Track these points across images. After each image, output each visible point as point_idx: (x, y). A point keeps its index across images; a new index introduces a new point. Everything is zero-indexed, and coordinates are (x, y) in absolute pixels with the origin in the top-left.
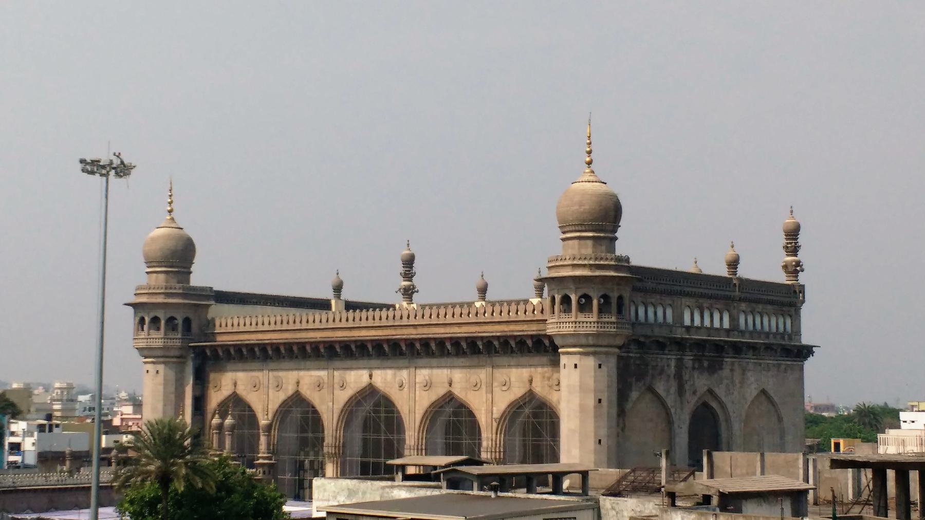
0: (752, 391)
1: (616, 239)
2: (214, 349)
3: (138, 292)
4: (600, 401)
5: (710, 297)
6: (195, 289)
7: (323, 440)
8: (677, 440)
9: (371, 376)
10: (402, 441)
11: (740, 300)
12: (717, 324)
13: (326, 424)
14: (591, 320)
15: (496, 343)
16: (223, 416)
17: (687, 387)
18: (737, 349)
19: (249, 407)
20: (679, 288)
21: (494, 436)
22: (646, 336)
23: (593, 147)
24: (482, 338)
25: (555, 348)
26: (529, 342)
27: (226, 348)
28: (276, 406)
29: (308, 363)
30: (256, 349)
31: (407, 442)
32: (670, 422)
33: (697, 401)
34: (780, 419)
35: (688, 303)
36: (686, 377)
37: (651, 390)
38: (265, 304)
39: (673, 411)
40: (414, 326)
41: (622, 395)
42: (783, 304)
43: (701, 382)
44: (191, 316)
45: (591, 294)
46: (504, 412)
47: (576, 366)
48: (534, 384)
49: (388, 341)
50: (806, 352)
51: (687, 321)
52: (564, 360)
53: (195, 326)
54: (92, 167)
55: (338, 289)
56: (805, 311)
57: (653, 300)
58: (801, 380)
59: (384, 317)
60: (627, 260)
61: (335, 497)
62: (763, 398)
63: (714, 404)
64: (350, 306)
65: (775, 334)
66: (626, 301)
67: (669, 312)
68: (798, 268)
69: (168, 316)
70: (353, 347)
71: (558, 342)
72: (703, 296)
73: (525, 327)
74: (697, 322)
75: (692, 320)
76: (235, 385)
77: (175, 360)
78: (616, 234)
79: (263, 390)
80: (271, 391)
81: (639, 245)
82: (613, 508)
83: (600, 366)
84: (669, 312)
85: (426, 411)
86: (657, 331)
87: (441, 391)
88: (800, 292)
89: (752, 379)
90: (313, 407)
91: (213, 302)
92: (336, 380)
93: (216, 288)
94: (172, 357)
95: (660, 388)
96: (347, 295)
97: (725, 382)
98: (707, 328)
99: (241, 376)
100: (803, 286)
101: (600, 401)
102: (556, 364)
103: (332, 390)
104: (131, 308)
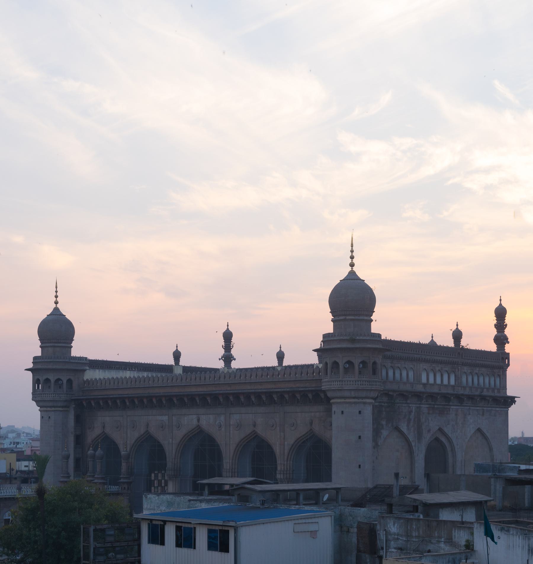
1: (372, 321)
3: (37, 361)
5: (441, 362)
6: (75, 358)
9: (198, 420)
11: (463, 364)
12: (446, 382)
13: (167, 454)
15: (286, 396)
16: (95, 450)
19: (114, 442)
21: (285, 463)
22: (394, 391)
24: (277, 392)
25: (328, 399)
26: (310, 396)
31: (225, 467)
37: (397, 429)
38: (125, 369)
39: (413, 444)
40: (229, 385)
41: (377, 432)
43: (433, 423)
44: (72, 378)
45: (353, 361)
46: (293, 445)
47: (342, 412)
49: (210, 395)
51: (424, 380)
52: (334, 408)
53: (75, 385)
56: (510, 371)
57: (399, 365)
60: (379, 335)
61: (159, 507)
63: (443, 439)
65: (488, 389)
67: (411, 374)
68: (505, 341)
69: (56, 378)
70: (186, 399)
71: (329, 394)
74: (431, 381)
75: (428, 379)
76: (104, 427)
79: (124, 429)
82: (351, 515)
83: (360, 412)
84: (411, 374)
85: (238, 445)
90: (159, 442)
91: (88, 368)
93: (91, 357)
94: (60, 407)
95: (404, 428)
96: (183, 362)
98: (438, 385)
100: (509, 354)
101: (360, 437)
102: (329, 412)
104: (30, 373)
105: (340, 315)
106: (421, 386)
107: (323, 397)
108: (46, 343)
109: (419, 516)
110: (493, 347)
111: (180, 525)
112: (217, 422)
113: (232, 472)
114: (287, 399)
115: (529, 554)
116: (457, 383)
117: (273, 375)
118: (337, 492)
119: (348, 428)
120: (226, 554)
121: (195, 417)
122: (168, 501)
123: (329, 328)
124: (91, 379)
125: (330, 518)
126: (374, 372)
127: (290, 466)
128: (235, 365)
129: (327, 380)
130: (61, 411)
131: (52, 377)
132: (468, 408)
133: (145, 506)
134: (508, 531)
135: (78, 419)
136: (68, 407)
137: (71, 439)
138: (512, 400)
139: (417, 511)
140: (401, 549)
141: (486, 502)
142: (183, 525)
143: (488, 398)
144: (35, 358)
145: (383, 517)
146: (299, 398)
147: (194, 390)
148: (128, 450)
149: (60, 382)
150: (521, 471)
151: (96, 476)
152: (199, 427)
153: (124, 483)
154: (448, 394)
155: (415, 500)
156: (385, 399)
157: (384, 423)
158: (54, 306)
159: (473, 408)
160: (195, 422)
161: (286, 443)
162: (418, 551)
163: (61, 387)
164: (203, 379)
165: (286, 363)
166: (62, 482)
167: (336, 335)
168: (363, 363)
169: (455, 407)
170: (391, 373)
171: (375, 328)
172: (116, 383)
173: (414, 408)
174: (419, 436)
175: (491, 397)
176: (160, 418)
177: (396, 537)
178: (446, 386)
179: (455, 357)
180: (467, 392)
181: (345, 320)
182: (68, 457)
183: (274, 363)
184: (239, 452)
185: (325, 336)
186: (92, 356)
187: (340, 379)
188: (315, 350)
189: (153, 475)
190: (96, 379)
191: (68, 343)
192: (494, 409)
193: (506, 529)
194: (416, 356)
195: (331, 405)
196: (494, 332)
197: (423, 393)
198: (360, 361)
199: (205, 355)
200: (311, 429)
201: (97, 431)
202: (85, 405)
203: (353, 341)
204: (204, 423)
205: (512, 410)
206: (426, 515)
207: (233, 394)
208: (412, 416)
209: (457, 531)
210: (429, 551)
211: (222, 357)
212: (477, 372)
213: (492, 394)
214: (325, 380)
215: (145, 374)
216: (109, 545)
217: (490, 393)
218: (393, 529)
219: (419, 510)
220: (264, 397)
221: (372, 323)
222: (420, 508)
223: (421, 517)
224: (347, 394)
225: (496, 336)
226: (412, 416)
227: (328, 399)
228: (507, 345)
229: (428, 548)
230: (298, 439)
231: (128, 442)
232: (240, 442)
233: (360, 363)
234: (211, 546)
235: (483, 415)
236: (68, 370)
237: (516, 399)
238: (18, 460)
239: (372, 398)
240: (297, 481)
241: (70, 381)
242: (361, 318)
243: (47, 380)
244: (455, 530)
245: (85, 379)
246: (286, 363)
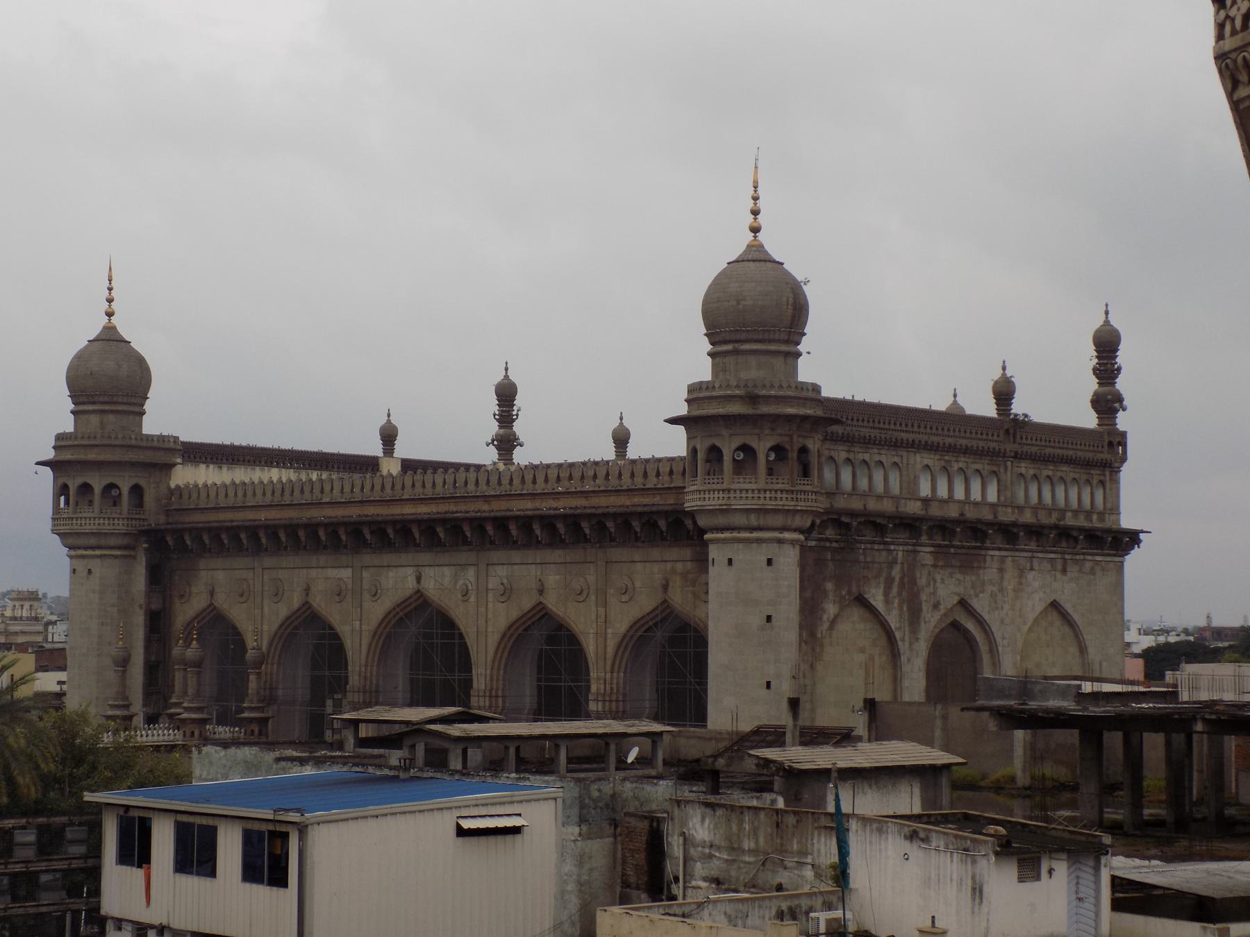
0: (1035, 604)
2: (179, 533)
3: (62, 443)
5: (966, 451)
6: (150, 438)
7: (347, 677)
8: (906, 683)
9: (419, 579)
10: (467, 684)
11: (1017, 456)
12: (976, 495)
13: (349, 654)
14: (754, 486)
15: (610, 524)
17: (924, 597)
18: (1010, 534)
19: (235, 628)
20: (911, 437)
21: (608, 675)
22: (853, 514)
23: (761, 204)
26: (662, 524)
27: (197, 532)
28: (275, 626)
29: (323, 559)
30: (243, 536)
31: (475, 685)
32: (894, 654)
33: (940, 620)
34: (1083, 650)
35: (926, 461)
36: (922, 581)
39: (898, 635)
42: (1088, 464)
43: (945, 589)
44: (142, 483)
45: (754, 445)
46: (625, 635)
47: (730, 561)
48: (670, 589)
49: (444, 521)
52: (713, 552)
53: (149, 498)
55: (389, 437)
56: (1128, 474)
57: (867, 457)
58: (1118, 586)
59: (439, 480)
60: (816, 388)
62: (1054, 616)
63: (970, 625)
64: (409, 466)
65: (1076, 513)
66: (814, 460)
67: (894, 478)
68: (1117, 405)
70: (390, 531)
71: (702, 522)
72: (951, 449)
73: (656, 499)
74: (943, 492)
75: (934, 489)
76: (212, 593)
77: (118, 553)
79: (254, 600)
80: (266, 602)
81: (834, 363)
83: (770, 562)
84: (894, 478)
85: (504, 635)
86: (873, 505)
87: (527, 603)
88: (1119, 444)
89: (1036, 584)
90: (331, 628)
91: (179, 460)
92: (366, 586)
93: (184, 438)
95: (876, 597)
96: (404, 449)
97: (989, 588)
98: (959, 502)
99: (220, 575)
100: (1124, 435)
101: (769, 618)
102: (702, 562)
103: (361, 599)
105: (725, 342)
106: (919, 504)
107: (690, 527)
108: (83, 403)
109: (774, 802)
110: (1088, 420)
111: (191, 819)
112: (461, 582)
113: (490, 696)
114: (612, 530)
115: (974, 899)
116: (1002, 498)
117: (583, 477)
118: (654, 742)
119: (747, 600)
120: (282, 890)
121: (410, 571)
122: (245, 762)
124: (187, 486)
125: (552, 803)
126: (806, 472)
127: (618, 684)
129: (695, 488)
130: (116, 557)
132: (1030, 554)
133: (197, 772)
134: (926, 840)
135: (156, 576)
136: (133, 548)
137: (139, 620)
138: (1130, 539)
139: (771, 791)
140: (717, 881)
141: (947, 767)
142: (198, 820)
143: (1075, 533)
144: (59, 437)
145: (678, 803)
146: (638, 529)
147: (408, 510)
148: (264, 649)
149: (114, 492)
150: (1081, 697)
151: (185, 705)
152: (419, 593)
153: (251, 720)
154: (979, 521)
155: (767, 762)
156: (830, 533)
157: (829, 586)
159: (1040, 555)
161: (609, 631)
162: (754, 887)
163: (116, 502)
164: (429, 485)
165: (633, 452)
166: (108, 718)
167: (717, 385)
168: (777, 449)
169: (997, 553)
170: (846, 476)
171: (806, 371)
172: (240, 494)
173: (900, 554)
174: (914, 616)
175: (1081, 530)
176: (333, 573)
177: (707, 851)
178: (976, 504)
179: (1002, 438)
180: (1028, 517)
181: (736, 352)
182: (123, 663)
183: (608, 452)
184: (506, 653)
185: (692, 389)
186: (191, 434)
187: (725, 486)
188: (673, 421)
189: (329, 703)
190: (196, 486)
191: (134, 404)
192: (1089, 558)
193: (922, 835)
194: (904, 436)
195: (705, 544)
196: (1092, 384)
197: (921, 519)
198: (769, 445)
199: (453, 432)
200: (665, 601)
201: (197, 603)
202: (170, 543)
203: (753, 399)
205: (1133, 561)
206: (793, 798)
207: (495, 519)
208: (896, 572)
209: (823, 839)
210: (779, 888)
211: (493, 441)
212: (1050, 473)
213: (1086, 524)
214: (692, 488)
216: (18, 868)
217: (1081, 522)
218: (700, 831)
219: (776, 787)
220: (561, 527)
221: (800, 360)
222: (778, 782)
223: (781, 803)
224: (740, 520)
225: (1096, 394)
226: (896, 572)
228: (1120, 414)
229: (778, 880)
230: (635, 623)
231: (265, 627)
232: (510, 628)
233: (772, 449)
234: (251, 873)
235: (1064, 571)
237: (1142, 536)
238: (44, 669)
239: (801, 531)
240: (637, 716)
241: (137, 491)
242: (773, 347)
243: (86, 488)
244: (819, 835)
245: (173, 485)
246: (633, 452)
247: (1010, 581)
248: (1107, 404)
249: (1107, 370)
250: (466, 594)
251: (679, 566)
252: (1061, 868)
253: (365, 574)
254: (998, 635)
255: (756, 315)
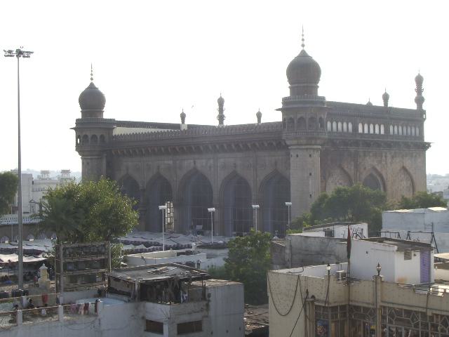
4: (310, 174)
18: (389, 146)
26: (274, 143)
38: (144, 127)
47: (297, 156)
50: (426, 146)
51: (360, 130)
52: (292, 153)
54: (9, 54)
55: (183, 116)
56: (426, 125)
60: (324, 98)
64: (189, 126)
67: (350, 126)
70: (185, 148)
76: (127, 170)
78: (318, 85)
79: (141, 170)
81: (330, 89)
83: (310, 155)
96: (187, 122)
101: (310, 174)
104: (74, 131)
121: (192, 161)
123: (287, 93)
128: (227, 123)
131: (89, 134)
135: (109, 165)
144: (77, 120)
152: (195, 168)
158: (90, 82)
160: (192, 165)
165: (263, 121)
171: (320, 93)
183: (255, 121)
186: (118, 119)
188: (277, 110)
195: (290, 149)
196: (415, 95)
204: (198, 165)
205: (428, 153)
215: (160, 130)
227: (287, 147)
236: (100, 128)
243: (86, 136)
247: (389, 160)
248: (420, 100)
249: (419, 91)
250: (210, 167)
251: (280, 158)
252: (418, 254)
253: (178, 162)
254: (385, 177)
255: (303, 73)
